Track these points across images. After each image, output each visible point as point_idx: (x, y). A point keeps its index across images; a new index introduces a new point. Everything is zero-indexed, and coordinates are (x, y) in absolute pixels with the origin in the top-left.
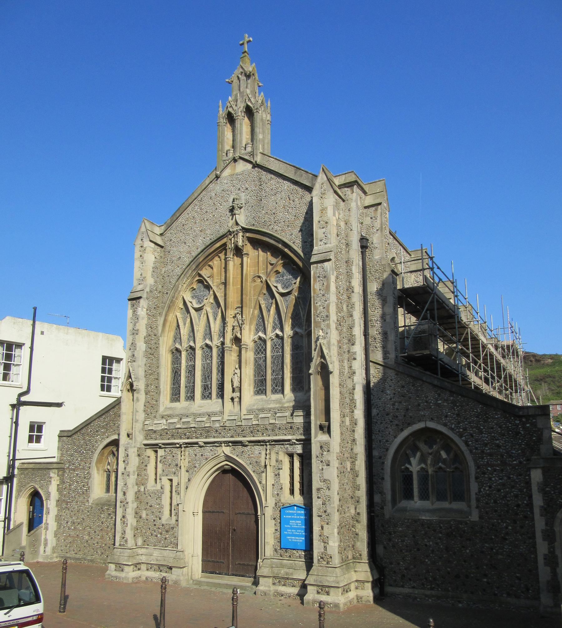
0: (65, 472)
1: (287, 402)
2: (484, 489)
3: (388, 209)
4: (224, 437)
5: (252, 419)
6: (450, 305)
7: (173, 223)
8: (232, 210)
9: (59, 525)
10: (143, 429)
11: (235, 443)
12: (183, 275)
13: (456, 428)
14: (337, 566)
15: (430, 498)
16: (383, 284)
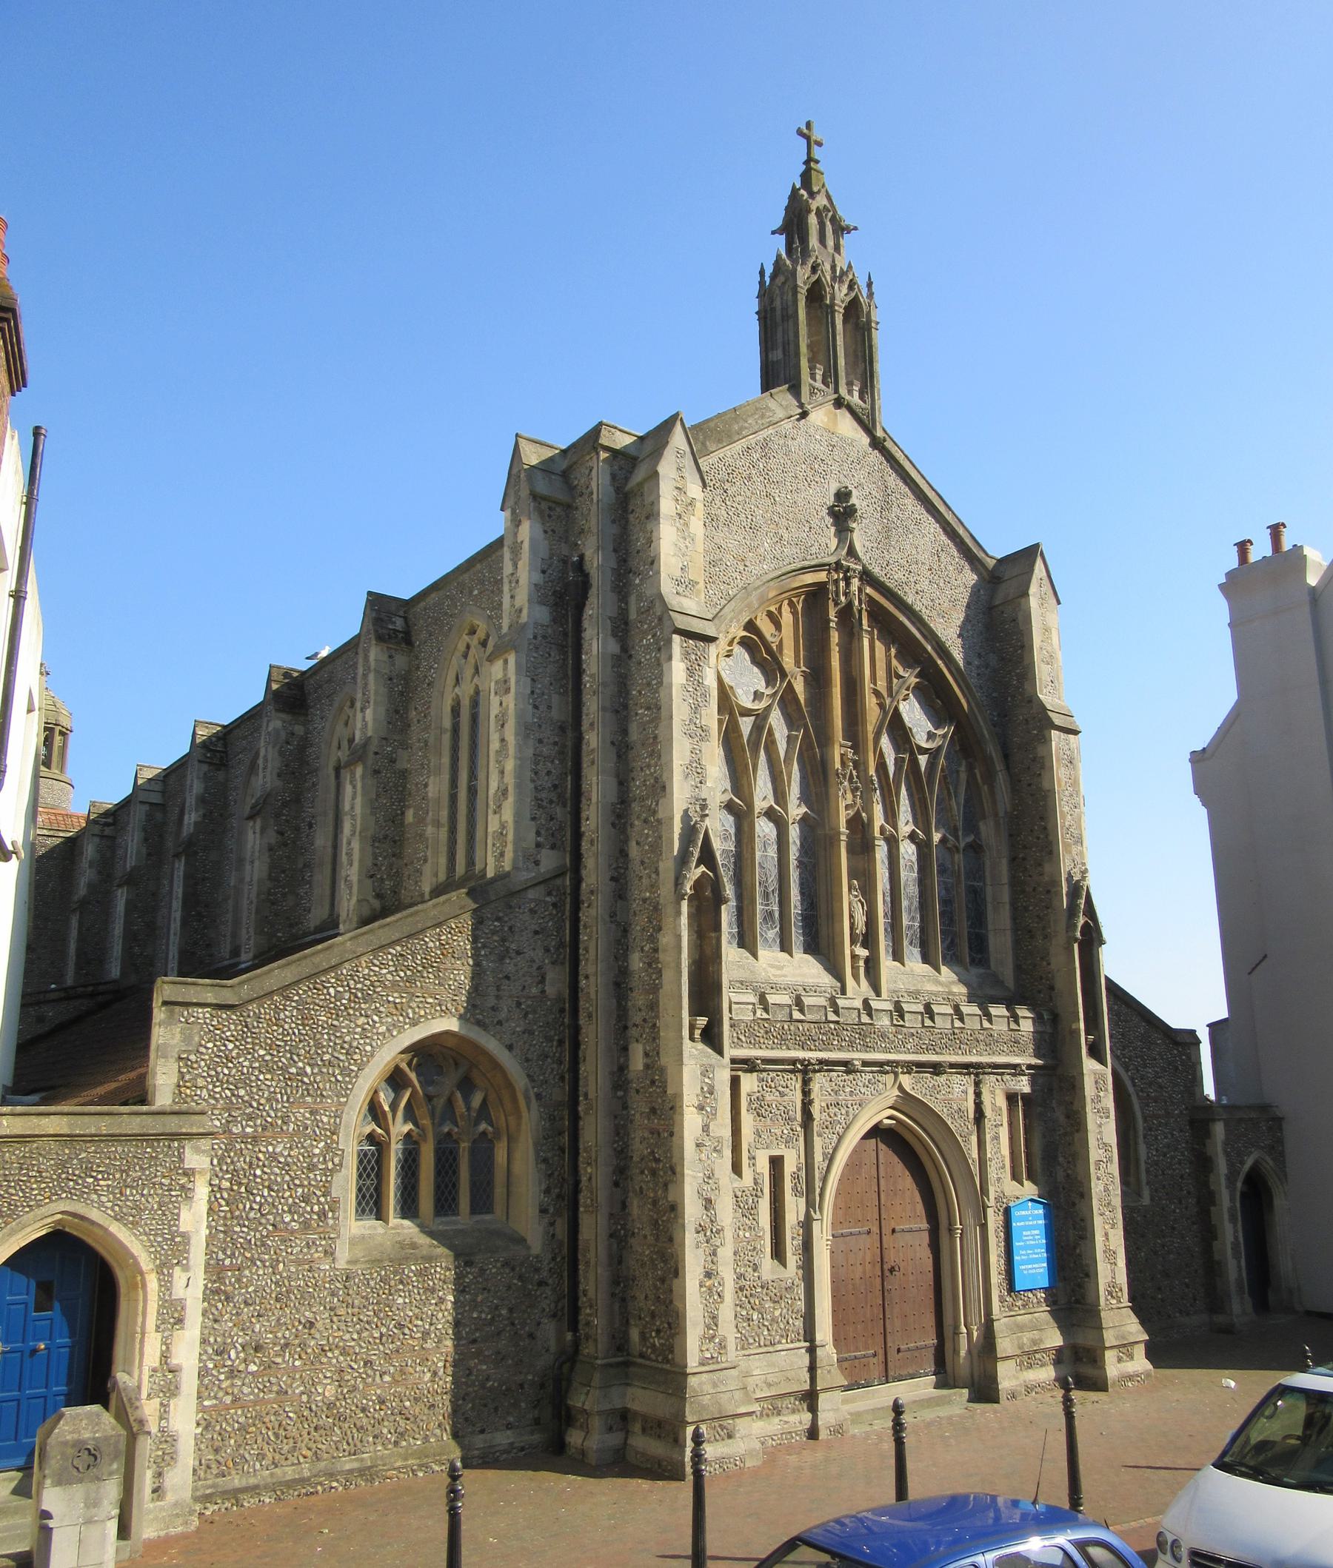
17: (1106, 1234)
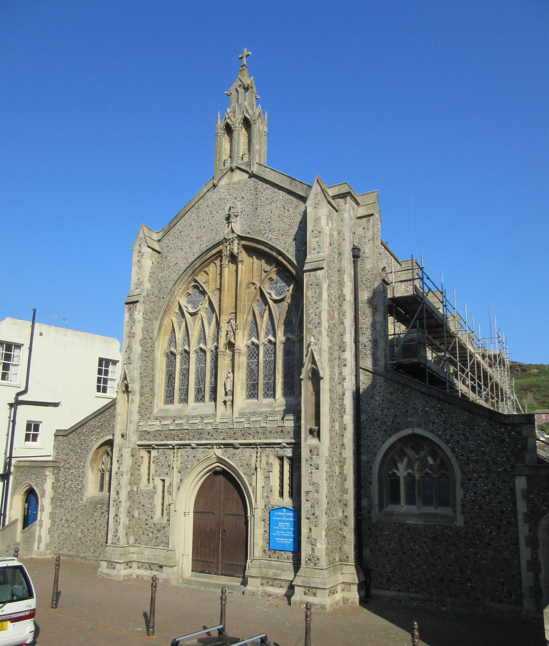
0: (60, 470)
1: (278, 406)
2: (470, 495)
3: (379, 220)
4: (216, 439)
5: (243, 422)
6: (439, 315)
7: (170, 230)
8: (228, 218)
9: (53, 523)
10: (137, 430)
11: (227, 445)
12: (179, 281)
13: (443, 435)
14: (324, 568)
15: (417, 503)
16: (374, 293)
17: (310, 530)
